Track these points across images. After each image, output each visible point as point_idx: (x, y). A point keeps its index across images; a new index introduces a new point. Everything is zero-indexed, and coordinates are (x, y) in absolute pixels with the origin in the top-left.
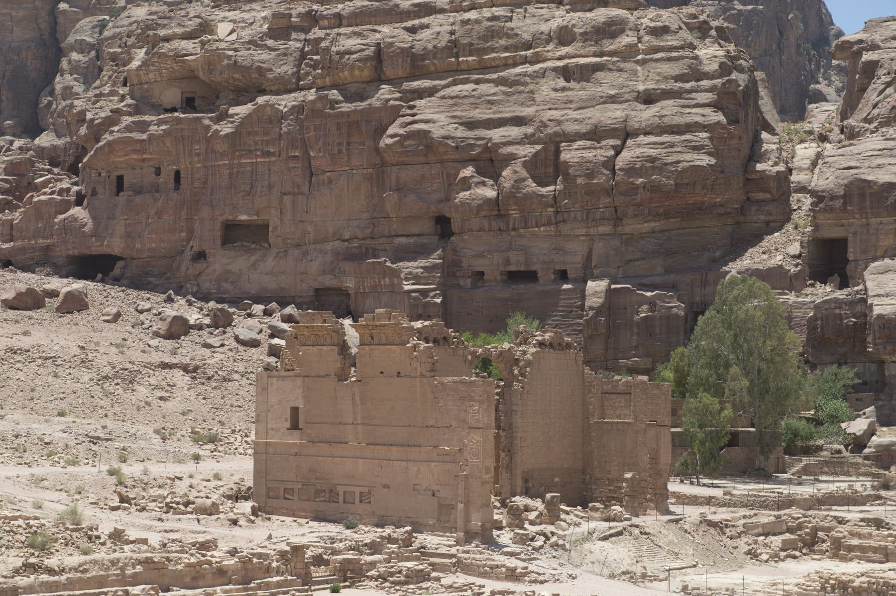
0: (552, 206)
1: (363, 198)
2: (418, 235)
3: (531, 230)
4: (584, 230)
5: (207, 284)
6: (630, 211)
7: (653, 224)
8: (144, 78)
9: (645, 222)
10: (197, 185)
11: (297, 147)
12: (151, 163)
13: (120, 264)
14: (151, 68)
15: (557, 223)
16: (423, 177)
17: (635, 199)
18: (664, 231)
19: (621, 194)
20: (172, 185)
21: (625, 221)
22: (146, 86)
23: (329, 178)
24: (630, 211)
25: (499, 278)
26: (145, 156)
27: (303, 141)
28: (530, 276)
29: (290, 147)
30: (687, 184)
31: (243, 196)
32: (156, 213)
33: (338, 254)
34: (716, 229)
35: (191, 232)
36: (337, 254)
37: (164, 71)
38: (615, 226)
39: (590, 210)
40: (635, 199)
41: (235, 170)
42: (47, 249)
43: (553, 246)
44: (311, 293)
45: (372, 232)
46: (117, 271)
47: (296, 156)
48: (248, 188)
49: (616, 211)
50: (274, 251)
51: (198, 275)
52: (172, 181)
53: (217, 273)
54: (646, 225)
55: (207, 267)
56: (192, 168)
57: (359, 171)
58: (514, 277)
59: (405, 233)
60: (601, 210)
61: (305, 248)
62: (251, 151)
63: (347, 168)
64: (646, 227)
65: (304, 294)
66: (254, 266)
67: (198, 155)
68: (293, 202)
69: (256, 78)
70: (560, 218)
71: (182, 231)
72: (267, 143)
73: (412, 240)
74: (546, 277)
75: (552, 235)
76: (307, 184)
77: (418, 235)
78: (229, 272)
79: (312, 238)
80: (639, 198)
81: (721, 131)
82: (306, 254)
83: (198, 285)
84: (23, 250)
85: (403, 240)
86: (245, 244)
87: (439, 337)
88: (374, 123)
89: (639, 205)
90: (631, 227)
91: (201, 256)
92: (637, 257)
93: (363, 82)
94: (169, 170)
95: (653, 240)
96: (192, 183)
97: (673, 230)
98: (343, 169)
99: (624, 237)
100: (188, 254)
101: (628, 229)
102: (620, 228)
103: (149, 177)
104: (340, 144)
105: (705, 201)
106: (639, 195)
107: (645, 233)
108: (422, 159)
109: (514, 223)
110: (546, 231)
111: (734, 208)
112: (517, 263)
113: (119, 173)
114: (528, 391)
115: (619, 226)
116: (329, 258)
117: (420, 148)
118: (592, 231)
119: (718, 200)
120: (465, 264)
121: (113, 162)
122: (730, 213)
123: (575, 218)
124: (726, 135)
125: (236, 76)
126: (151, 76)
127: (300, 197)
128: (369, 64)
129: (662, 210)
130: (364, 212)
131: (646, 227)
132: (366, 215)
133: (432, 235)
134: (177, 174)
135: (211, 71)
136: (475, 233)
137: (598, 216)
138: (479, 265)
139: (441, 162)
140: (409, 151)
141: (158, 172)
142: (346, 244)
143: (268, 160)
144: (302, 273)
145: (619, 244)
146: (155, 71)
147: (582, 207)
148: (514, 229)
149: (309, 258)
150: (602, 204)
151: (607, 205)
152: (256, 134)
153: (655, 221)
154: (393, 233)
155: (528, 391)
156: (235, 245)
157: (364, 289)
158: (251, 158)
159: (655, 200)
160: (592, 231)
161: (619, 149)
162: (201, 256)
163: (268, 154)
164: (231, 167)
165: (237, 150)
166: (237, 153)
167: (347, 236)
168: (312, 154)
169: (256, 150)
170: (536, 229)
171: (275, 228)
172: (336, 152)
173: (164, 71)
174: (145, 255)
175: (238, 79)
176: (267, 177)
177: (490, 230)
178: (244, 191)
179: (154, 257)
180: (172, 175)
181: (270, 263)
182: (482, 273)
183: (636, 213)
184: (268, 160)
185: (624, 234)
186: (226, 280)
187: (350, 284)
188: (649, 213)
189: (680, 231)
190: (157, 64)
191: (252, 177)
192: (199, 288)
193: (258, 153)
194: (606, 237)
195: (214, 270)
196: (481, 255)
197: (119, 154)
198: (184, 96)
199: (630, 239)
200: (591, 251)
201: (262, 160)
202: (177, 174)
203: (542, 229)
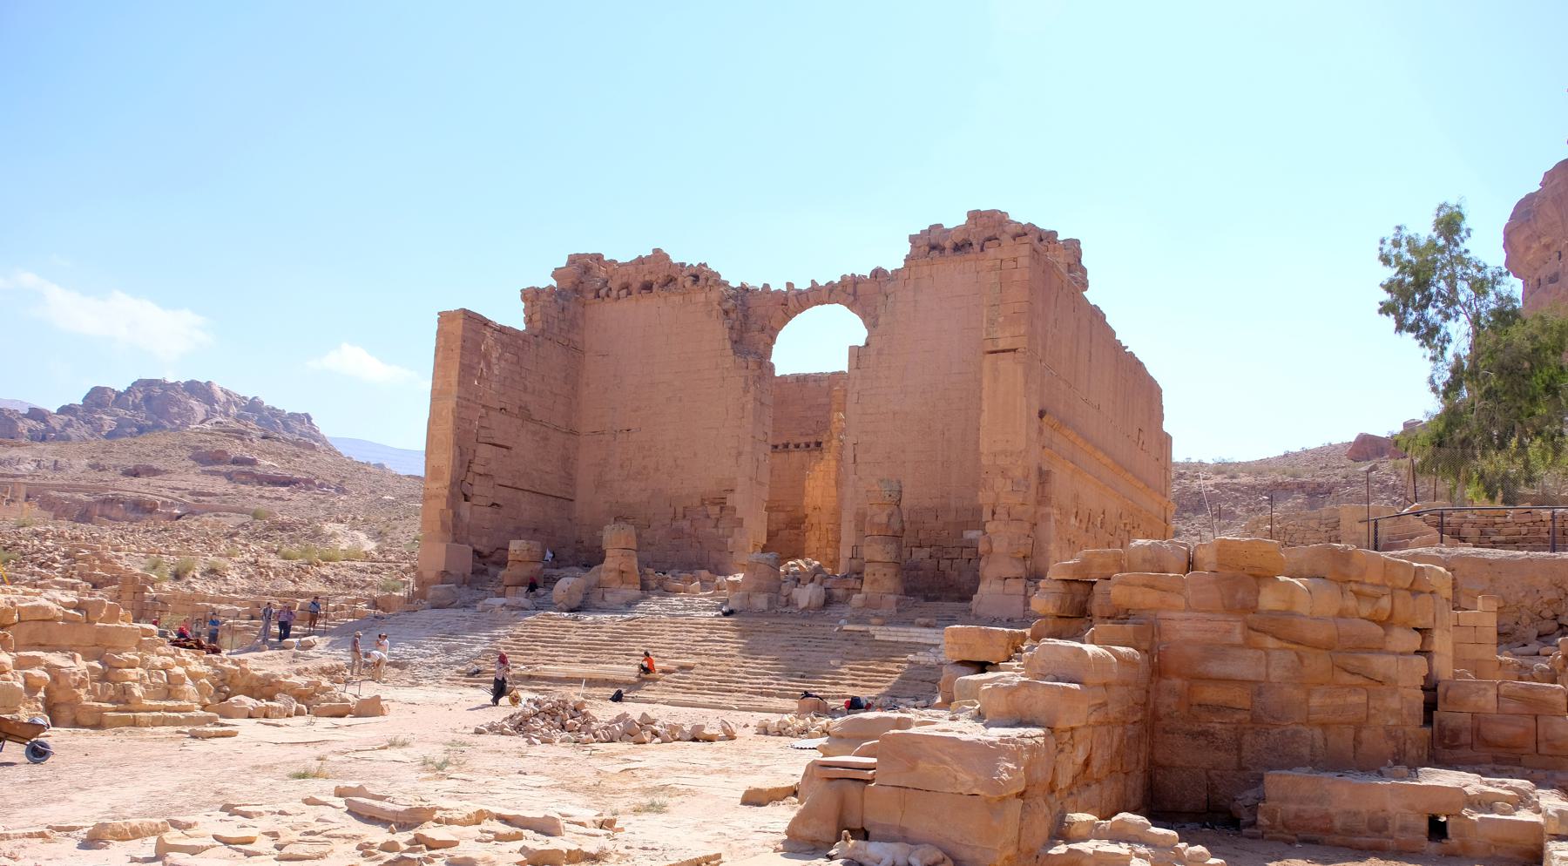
26: (1544, 240)
87: (653, 278)
113: (1536, 277)
155: (880, 353)
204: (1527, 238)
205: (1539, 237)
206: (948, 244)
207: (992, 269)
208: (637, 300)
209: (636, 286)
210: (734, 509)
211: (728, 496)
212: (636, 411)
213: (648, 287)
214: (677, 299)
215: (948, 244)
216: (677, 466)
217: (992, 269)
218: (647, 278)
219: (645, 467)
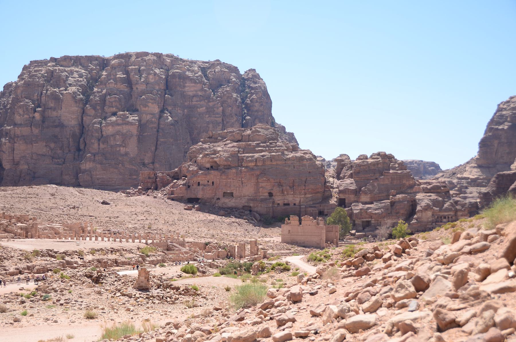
13: (200, 200)
20: (212, 184)
24: (308, 193)
28: (288, 204)
35: (216, 194)
36: (248, 199)
46: (200, 201)
58: (285, 205)
64: (310, 196)
66: (230, 201)
82: (241, 199)
84: (177, 197)
91: (219, 199)
94: (211, 182)
100: (215, 198)
101: (307, 196)
103: (206, 182)
112: (286, 202)
116: (246, 200)
120: (276, 202)
131: (310, 196)
134: (213, 182)
138: (279, 202)
141: (208, 182)
163: (234, 179)
164: (226, 181)
181: (234, 200)
182: (279, 204)
187: (251, 205)
199: (307, 198)
200: (300, 200)
202: (213, 182)
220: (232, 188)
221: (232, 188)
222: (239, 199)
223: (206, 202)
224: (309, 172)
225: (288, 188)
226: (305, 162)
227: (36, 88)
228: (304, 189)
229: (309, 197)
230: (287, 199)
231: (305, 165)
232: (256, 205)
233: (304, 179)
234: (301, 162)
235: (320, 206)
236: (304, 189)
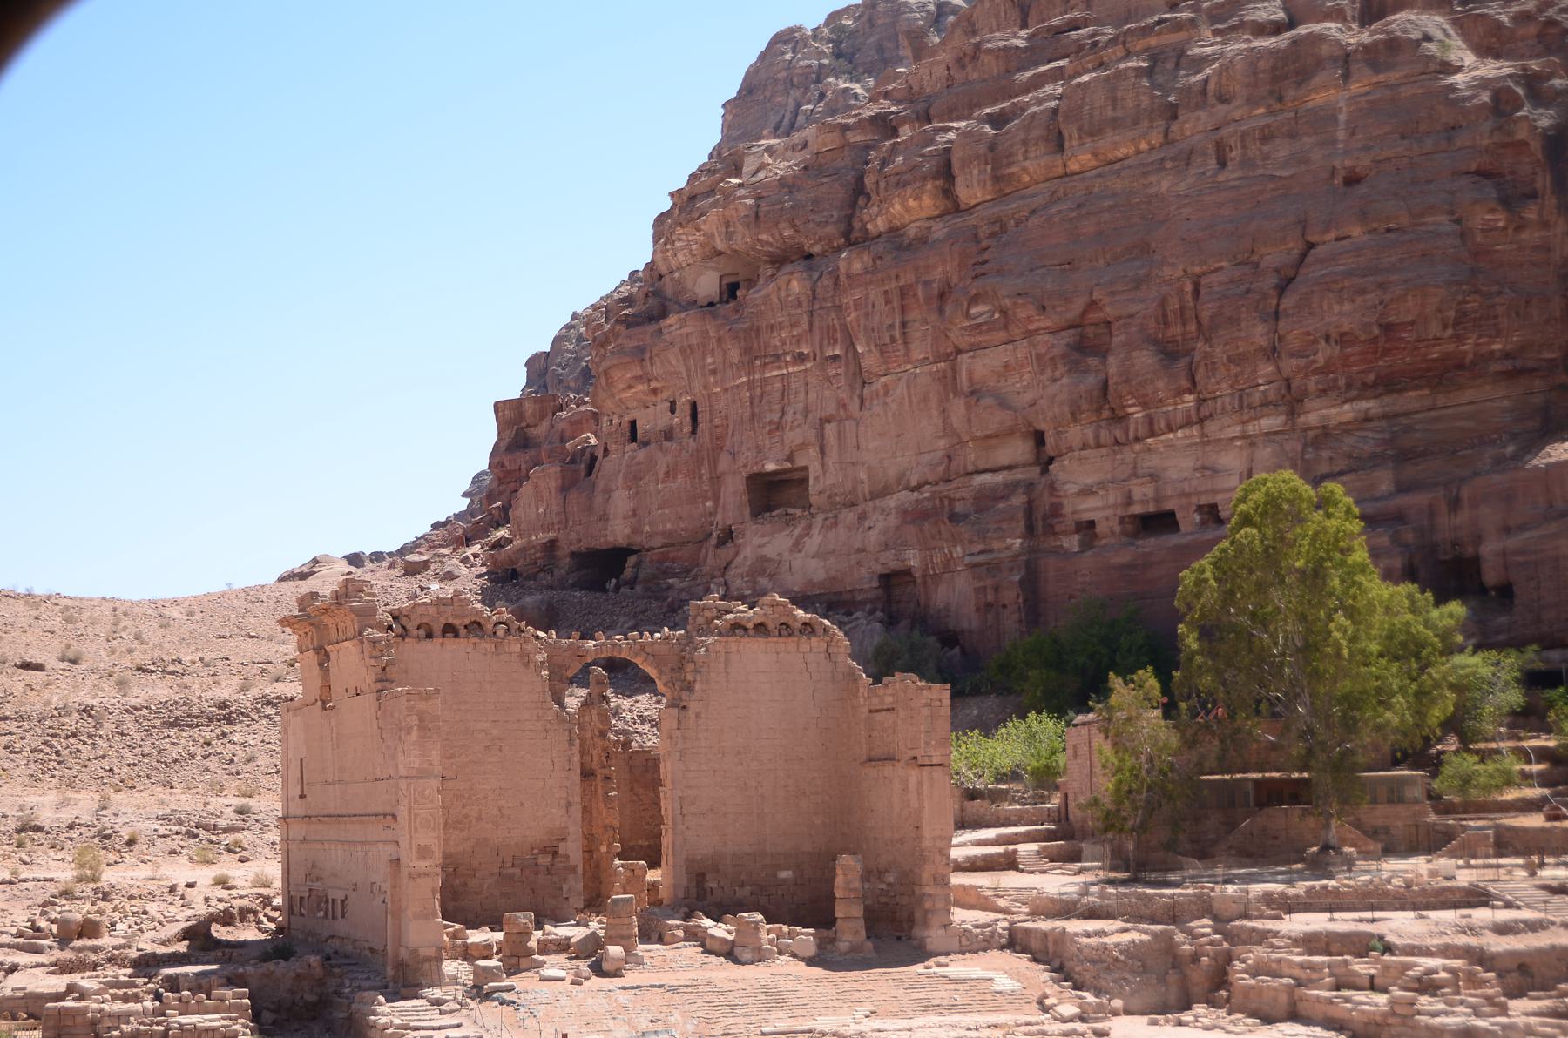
0: (1190, 393)
1: (935, 413)
2: (1009, 468)
3: (1163, 437)
4: (1238, 428)
5: (739, 582)
6: (1312, 384)
7: (1364, 405)
8: (674, 264)
9: (1345, 402)
10: (717, 421)
11: (835, 341)
12: (665, 395)
13: (632, 560)
14: (678, 244)
15: (1201, 421)
16: (1006, 366)
17: (1314, 362)
18: (1396, 415)
19: (1292, 355)
20: (687, 429)
21: (1308, 404)
22: (677, 275)
23: (885, 386)
25: (1117, 529)
26: (654, 385)
27: (846, 330)
29: (826, 342)
30: (1412, 323)
31: (770, 432)
32: (667, 474)
33: (905, 512)
34: (1506, 403)
37: (694, 247)
38: (1292, 413)
39: (1242, 390)
40: (1314, 362)
41: (758, 391)
42: (551, 545)
43: (1199, 463)
44: (875, 584)
45: (948, 468)
47: (835, 357)
48: (776, 417)
49: (1289, 387)
50: (820, 518)
51: (725, 568)
52: (688, 419)
53: (748, 563)
54: (1347, 407)
55: (737, 554)
56: (709, 396)
57: (926, 369)
59: (987, 466)
60: (1262, 388)
61: (859, 509)
62: (777, 357)
63: (909, 366)
64: (1347, 412)
65: (866, 586)
66: (797, 546)
67: (714, 372)
68: (839, 432)
69: (791, 237)
70: (1205, 411)
71: (706, 499)
72: (798, 340)
73: (999, 478)
74: (1189, 520)
75: (1196, 444)
76: (857, 400)
77: (1009, 468)
78: (763, 559)
79: (867, 490)
80: (1321, 359)
81: (1488, 217)
82: (862, 517)
83: (726, 584)
85: (987, 478)
86: (790, 510)
87: (457, 622)
88: (935, 285)
89: (1324, 370)
90: (1315, 414)
92: (1337, 469)
93: (929, 218)
94: (683, 401)
95: (1370, 435)
96: (711, 421)
97: (1417, 412)
98: (903, 368)
99: (1311, 434)
101: (1312, 418)
102: (1302, 419)
104: (891, 326)
105: (1466, 352)
106: (1320, 354)
107: (1349, 423)
108: (1003, 335)
109: (1136, 430)
110: (1186, 437)
111: (1545, 360)
112: (1143, 498)
113: (628, 418)
114: (698, 716)
115: (1299, 415)
116: (893, 520)
117: (997, 316)
118: (1251, 429)
119: (1496, 347)
120: (1067, 510)
121: (620, 400)
122: (1534, 370)
123: (1224, 409)
124: (1501, 224)
125: (764, 237)
126: (681, 257)
127: (847, 423)
128: (929, 186)
129: (1371, 377)
130: (941, 437)
131: (1347, 412)
132: (942, 443)
133: (1030, 465)
134: (694, 406)
135: (729, 235)
136: (1076, 453)
137: (1256, 397)
138: (1089, 508)
139: (1029, 334)
140: (980, 325)
142: (916, 494)
143: (803, 368)
144: (860, 551)
145: (1299, 448)
146: (682, 248)
147: (1232, 386)
148: (1137, 440)
149: (867, 524)
150: (1262, 376)
151: (1271, 378)
152: (781, 326)
153: (1366, 398)
154: (970, 468)
155: (698, 716)
156: (774, 513)
157: (933, 569)
158: (779, 368)
159: (1352, 359)
160: (1251, 429)
161: (1291, 273)
162: (728, 536)
163: (801, 358)
164: (750, 385)
165: (756, 358)
166: (758, 363)
167: (914, 483)
168: (860, 350)
169: (785, 354)
170: (1171, 436)
171: (816, 479)
172: (887, 340)
173: (694, 247)
174: (657, 541)
175: (767, 243)
176: (802, 396)
177: (1098, 446)
178: (771, 423)
179: (673, 545)
180: (688, 411)
182: (1091, 524)
183: (1321, 387)
184: (803, 368)
185: (1311, 429)
186: (763, 572)
187: (913, 560)
188: (1349, 386)
189: (1433, 413)
190: (684, 237)
191: (782, 399)
192: (728, 589)
193: (788, 358)
194: (1278, 438)
195: (745, 557)
196: (1086, 492)
197: (622, 386)
198: (724, 282)
199: (1324, 435)
201: (796, 369)
202: (694, 406)
203: (1180, 434)
204: (636, 378)
205: (650, 380)
206: (750, 625)
207: (925, 705)
208: (442, 644)
209: (437, 628)
210: (567, 857)
211: (561, 844)
212: (450, 758)
213: (450, 630)
214: (487, 645)
215: (750, 625)
216: (502, 816)
217: (925, 705)
218: (450, 620)
219: (466, 816)
220: (793, 437)
221: (793, 437)
222: (848, 516)
223: (667, 573)
224: (1352, 180)
225: (1145, 359)
226: (1326, 94)
227: (780, 99)
228: (1272, 353)
229: (1347, 429)
230: (1154, 477)
231: (1326, 117)
232: (938, 559)
233: (1275, 256)
234: (1290, 94)
235: (1455, 504)
236: (1272, 353)
